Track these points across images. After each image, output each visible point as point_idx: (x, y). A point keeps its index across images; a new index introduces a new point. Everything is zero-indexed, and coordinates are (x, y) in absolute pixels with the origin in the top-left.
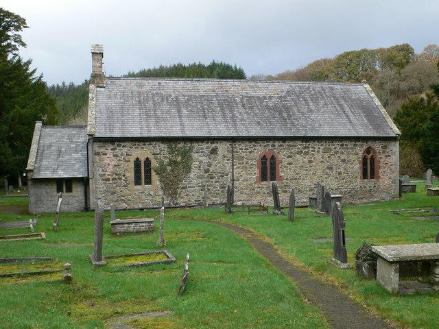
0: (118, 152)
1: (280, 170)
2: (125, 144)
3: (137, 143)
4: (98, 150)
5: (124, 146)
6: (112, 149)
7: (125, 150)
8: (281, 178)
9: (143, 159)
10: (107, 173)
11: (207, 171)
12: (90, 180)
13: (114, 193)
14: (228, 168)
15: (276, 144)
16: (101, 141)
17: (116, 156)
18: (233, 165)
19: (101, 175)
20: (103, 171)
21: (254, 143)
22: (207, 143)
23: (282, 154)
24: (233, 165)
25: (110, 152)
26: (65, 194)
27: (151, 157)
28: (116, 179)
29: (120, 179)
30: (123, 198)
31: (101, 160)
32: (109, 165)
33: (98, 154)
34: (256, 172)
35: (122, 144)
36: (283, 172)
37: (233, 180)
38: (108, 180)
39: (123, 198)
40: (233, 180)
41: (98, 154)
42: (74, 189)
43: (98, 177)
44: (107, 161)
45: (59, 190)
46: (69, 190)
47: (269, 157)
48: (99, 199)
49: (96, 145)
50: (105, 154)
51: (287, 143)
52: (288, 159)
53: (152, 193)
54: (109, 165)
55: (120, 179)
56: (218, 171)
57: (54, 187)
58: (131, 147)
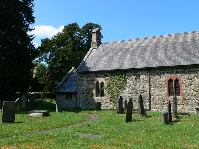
0: (89, 79)
1: (183, 88)
2: (92, 75)
3: (97, 74)
4: (80, 78)
5: (91, 76)
6: (86, 78)
7: (92, 78)
8: (184, 95)
9: (100, 83)
10: (84, 90)
11: (134, 89)
12: (77, 93)
13: (87, 100)
14: (147, 87)
15: (179, 71)
16: (81, 74)
17: (88, 81)
18: (150, 85)
19: (81, 91)
20: (82, 88)
21: (163, 71)
22: (134, 72)
23: (184, 78)
24: (150, 85)
25: (85, 79)
26: (69, 100)
27: (104, 82)
28: (88, 93)
29: (90, 93)
30: (91, 103)
31: (82, 83)
32: (85, 86)
33: (80, 80)
34: (166, 89)
35: (91, 75)
36: (183, 89)
37: (150, 95)
38: (84, 93)
39: (91, 103)
40: (150, 95)
41: (80, 80)
42: (73, 98)
43: (80, 92)
44: (84, 84)
45: (67, 98)
46: (71, 98)
47: (174, 80)
48: (81, 103)
49: (80, 76)
50: (83, 80)
51: (187, 70)
52: (189, 81)
53: (104, 101)
54: (85, 86)
55: (90, 93)
56: (141, 89)
57: (65, 96)
58: (95, 76)
